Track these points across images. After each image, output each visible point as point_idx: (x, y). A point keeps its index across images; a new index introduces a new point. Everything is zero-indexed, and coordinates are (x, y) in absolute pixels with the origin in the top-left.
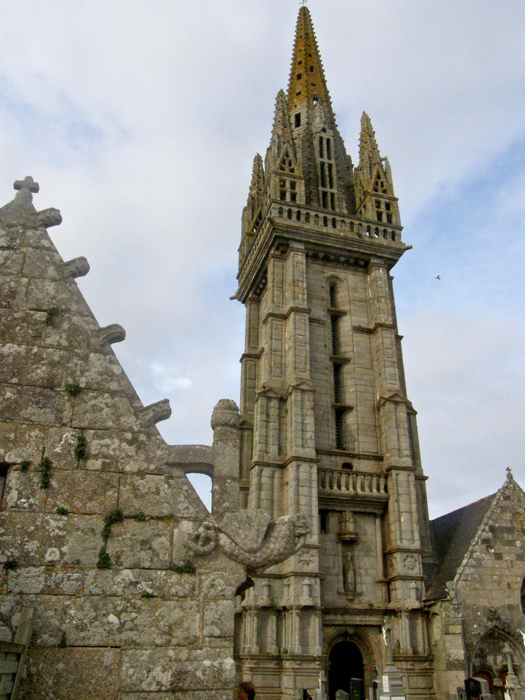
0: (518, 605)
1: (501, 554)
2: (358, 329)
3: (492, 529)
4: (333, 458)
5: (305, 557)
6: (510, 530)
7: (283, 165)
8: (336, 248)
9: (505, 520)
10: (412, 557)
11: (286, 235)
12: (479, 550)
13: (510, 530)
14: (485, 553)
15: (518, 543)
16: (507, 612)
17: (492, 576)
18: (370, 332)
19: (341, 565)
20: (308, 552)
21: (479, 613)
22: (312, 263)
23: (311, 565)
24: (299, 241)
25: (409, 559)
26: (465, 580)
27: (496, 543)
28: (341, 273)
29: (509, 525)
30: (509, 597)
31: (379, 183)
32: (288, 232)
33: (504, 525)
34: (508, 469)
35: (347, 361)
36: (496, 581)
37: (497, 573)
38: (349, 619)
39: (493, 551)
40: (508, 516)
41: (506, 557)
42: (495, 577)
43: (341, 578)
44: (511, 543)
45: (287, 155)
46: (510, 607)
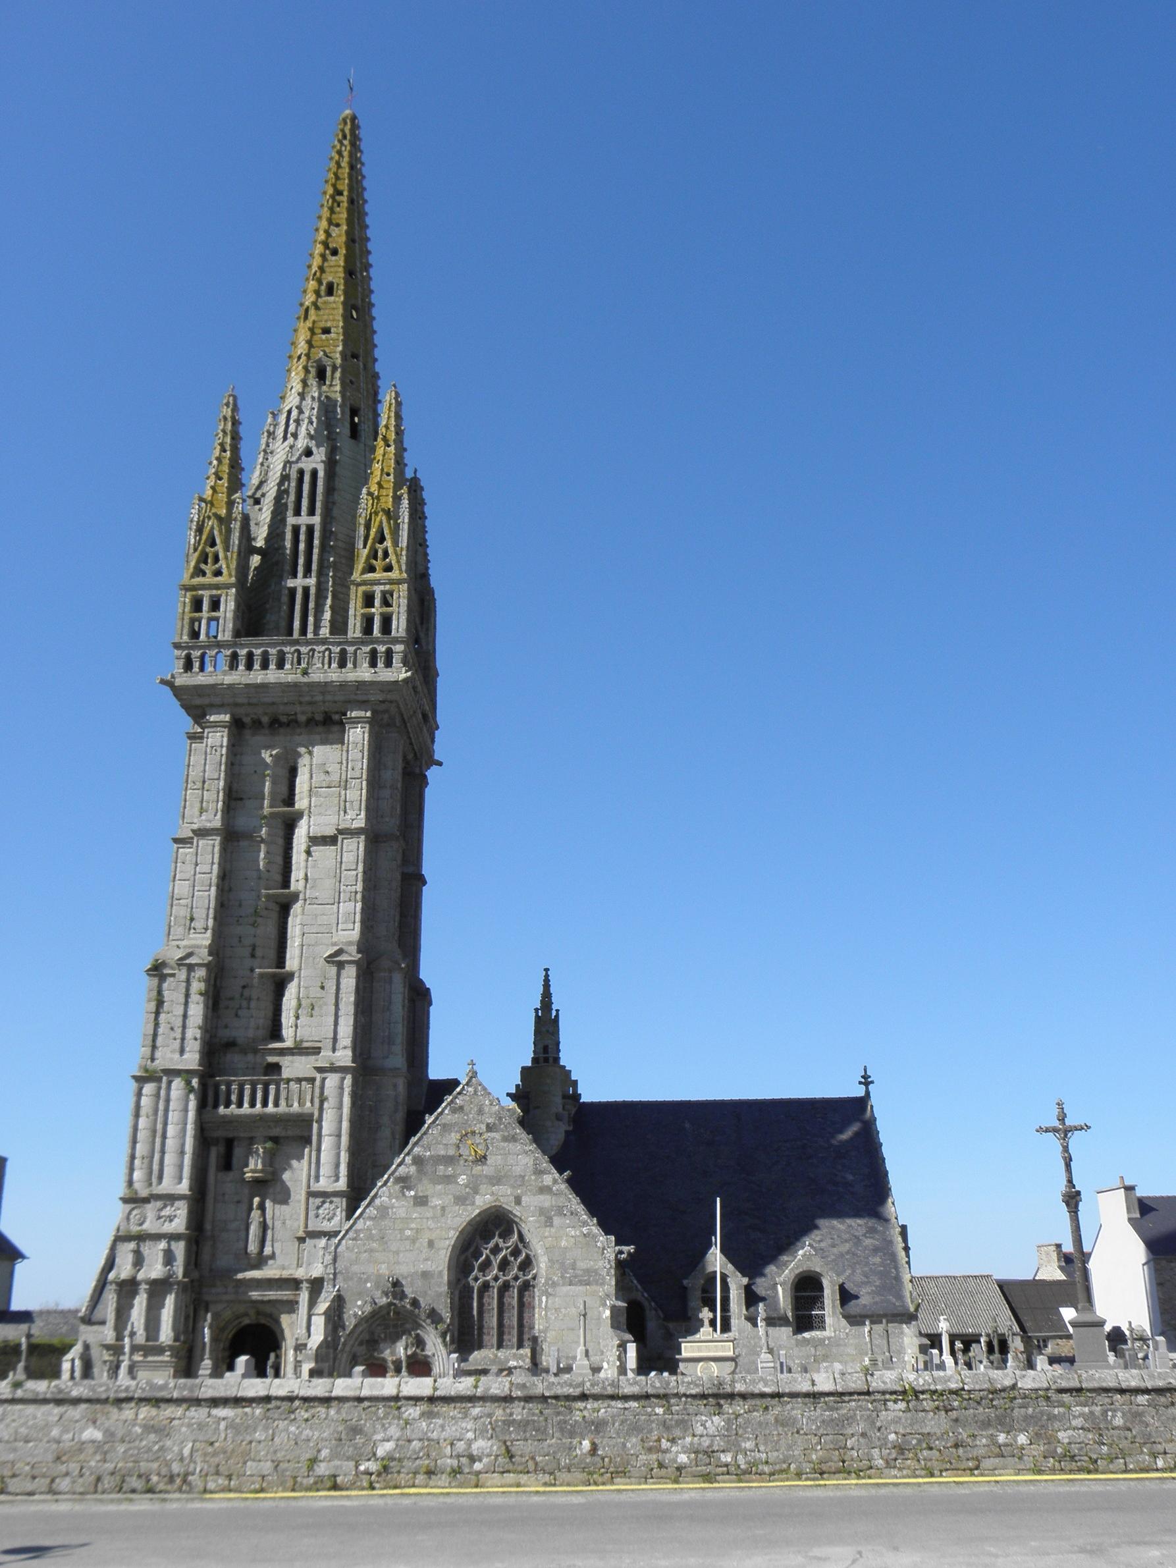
0: (440, 1272)
1: (426, 1197)
3: (418, 1161)
5: (167, 1212)
6: (449, 1160)
7: (203, 566)
9: (446, 1145)
12: (387, 1194)
13: (449, 1160)
14: (397, 1198)
15: (462, 1180)
16: (419, 1283)
17: (402, 1231)
20: (172, 1205)
21: (369, 1285)
22: (253, 735)
23: (176, 1220)
25: (327, 1205)
26: (354, 1239)
27: (421, 1180)
30: (427, 1260)
31: (380, 554)
33: (442, 1153)
35: (295, 897)
36: (408, 1238)
37: (413, 1226)
39: (412, 1193)
41: (436, 1202)
42: (408, 1233)
44: (449, 1179)
45: (213, 544)
46: (425, 1275)
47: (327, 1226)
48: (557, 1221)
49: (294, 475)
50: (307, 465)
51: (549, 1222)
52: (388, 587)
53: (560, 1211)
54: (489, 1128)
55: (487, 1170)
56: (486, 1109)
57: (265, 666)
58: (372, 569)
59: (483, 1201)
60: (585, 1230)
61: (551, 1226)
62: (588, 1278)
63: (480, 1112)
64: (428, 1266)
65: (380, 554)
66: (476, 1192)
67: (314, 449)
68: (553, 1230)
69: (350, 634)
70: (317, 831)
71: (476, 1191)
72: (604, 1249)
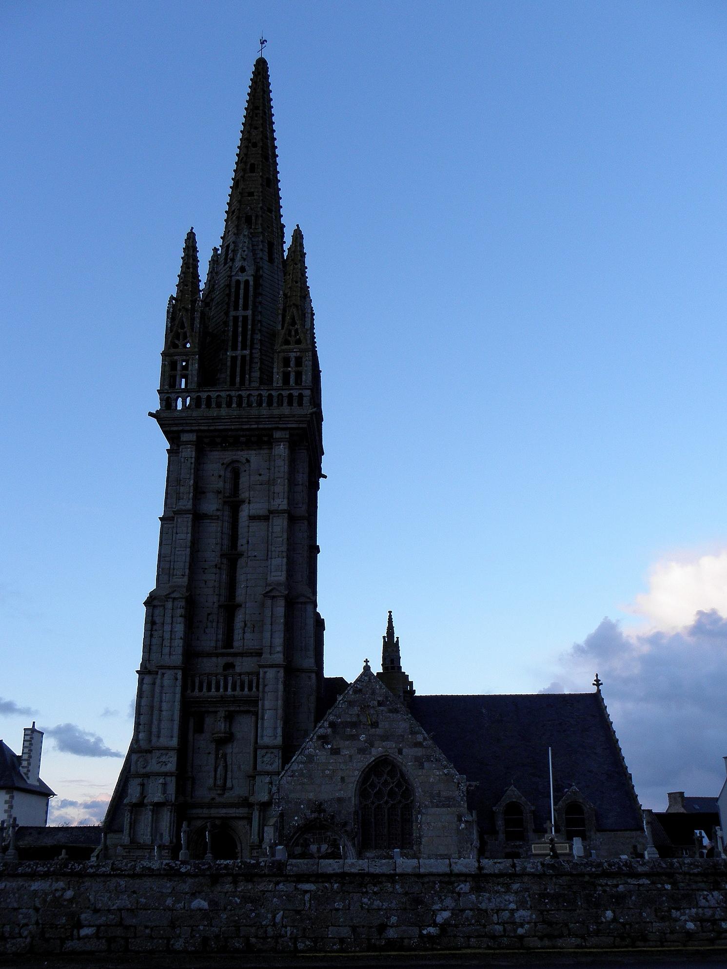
2: (252, 518)
3: (332, 725)
4: (214, 659)
5: (163, 759)
6: (354, 725)
8: (231, 430)
10: (272, 753)
11: (175, 429)
13: (354, 725)
15: (363, 737)
17: (323, 771)
18: (266, 518)
19: (213, 761)
20: (166, 754)
23: (169, 765)
24: (191, 431)
25: (269, 755)
28: (242, 455)
29: (354, 719)
31: (293, 333)
32: (176, 425)
34: (367, 661)
38: (214, 812)
39: (329, 746)
40: (356, 710)
42: (327, 772)
43: (212, 774)
44: (354, 737)
45: (183, 327)
46: (340, 800)
47: (269, 768)
48: (426, 765)
49: (233, 284)
50: (242, 278)
51: (421, 766)
52: (298, 354)
53: (428, 759)
54: (380, 704)
55: (379, 731)
56: (377, 691)
57: (219, 406)
58: (287, 342)
59: (377, 751)
60: (445, 771)
61: (423, 768)
62: (448, 802)
63: (373, 693)
64: (341, 794)
65: (293, 333)
66: (372, 745)
67: (247, 268)
68: (424, 771)
69: (275, 384)
70: (253, 512)
71: (372, 745)
72: (459, 783)
